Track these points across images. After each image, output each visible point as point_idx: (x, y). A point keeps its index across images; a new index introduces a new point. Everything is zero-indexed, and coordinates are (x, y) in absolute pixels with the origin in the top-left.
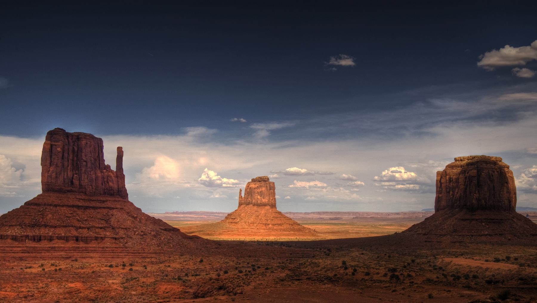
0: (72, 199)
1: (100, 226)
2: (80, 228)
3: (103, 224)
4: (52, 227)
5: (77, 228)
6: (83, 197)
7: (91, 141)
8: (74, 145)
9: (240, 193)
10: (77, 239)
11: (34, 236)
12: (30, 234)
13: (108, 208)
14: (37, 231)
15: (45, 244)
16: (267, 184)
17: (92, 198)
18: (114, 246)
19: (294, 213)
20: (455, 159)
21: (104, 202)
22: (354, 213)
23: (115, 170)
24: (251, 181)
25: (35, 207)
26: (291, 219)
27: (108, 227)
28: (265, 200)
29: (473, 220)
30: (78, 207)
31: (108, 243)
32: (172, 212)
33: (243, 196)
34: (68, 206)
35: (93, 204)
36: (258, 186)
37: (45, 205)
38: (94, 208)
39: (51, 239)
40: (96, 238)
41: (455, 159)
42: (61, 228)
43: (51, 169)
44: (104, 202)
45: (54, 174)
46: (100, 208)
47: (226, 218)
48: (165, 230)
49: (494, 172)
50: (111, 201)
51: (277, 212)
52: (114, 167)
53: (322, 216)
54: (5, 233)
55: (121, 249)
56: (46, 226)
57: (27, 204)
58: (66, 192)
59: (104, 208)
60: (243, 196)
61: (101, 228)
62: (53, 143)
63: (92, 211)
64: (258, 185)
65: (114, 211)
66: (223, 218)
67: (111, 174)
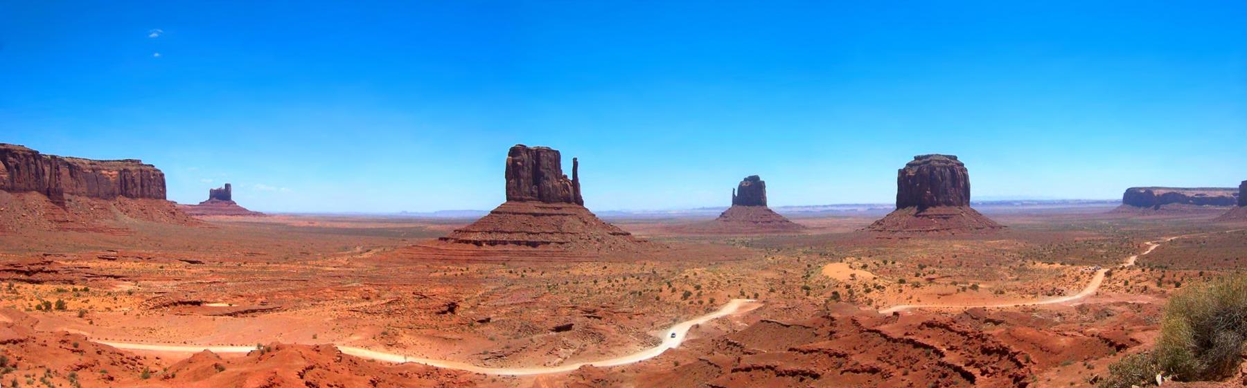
1: (550, 231)
2: (533, 233)
4: (505, 232)
5: (529, 233)
6: (541, 204)
9: (734, 192)
10: (528, 244)
11: (490, 241)
12: (488, 239)
13: (563, 215)
14: (494, 236)
15: (499, 247)
18: (557, 249)
19: (813, 207)
20: (915, 157)
21: (558, 209)
22: (869, 205)
23: (571, 179)
25: (498, 215)
26: (781, 216)
27: (557, 232)
29: (924, 216)
30: (535, 215)
31: (551, 248)
32: (699, 207)
35: (549, 211)
37: (507, 213)
38: (549, 215)
39: (505, 243)
40: (543, 243)
41: (915, 157)
43: (513, 181)
44: (558, 209)
46: (555, 215)
47: (721, 216)
48: (614, 234)
49: (946, 171)
52: (570, 178)
53: (839, 209)
54: (468, 238)
55: (560, 253)
56: (502, 232)
57: (492, 212)
59: (559, 214)
61: (550, 233)
63: (548, 217)
65: (567, 217)
66: (718, 217)
67: (568, 184)
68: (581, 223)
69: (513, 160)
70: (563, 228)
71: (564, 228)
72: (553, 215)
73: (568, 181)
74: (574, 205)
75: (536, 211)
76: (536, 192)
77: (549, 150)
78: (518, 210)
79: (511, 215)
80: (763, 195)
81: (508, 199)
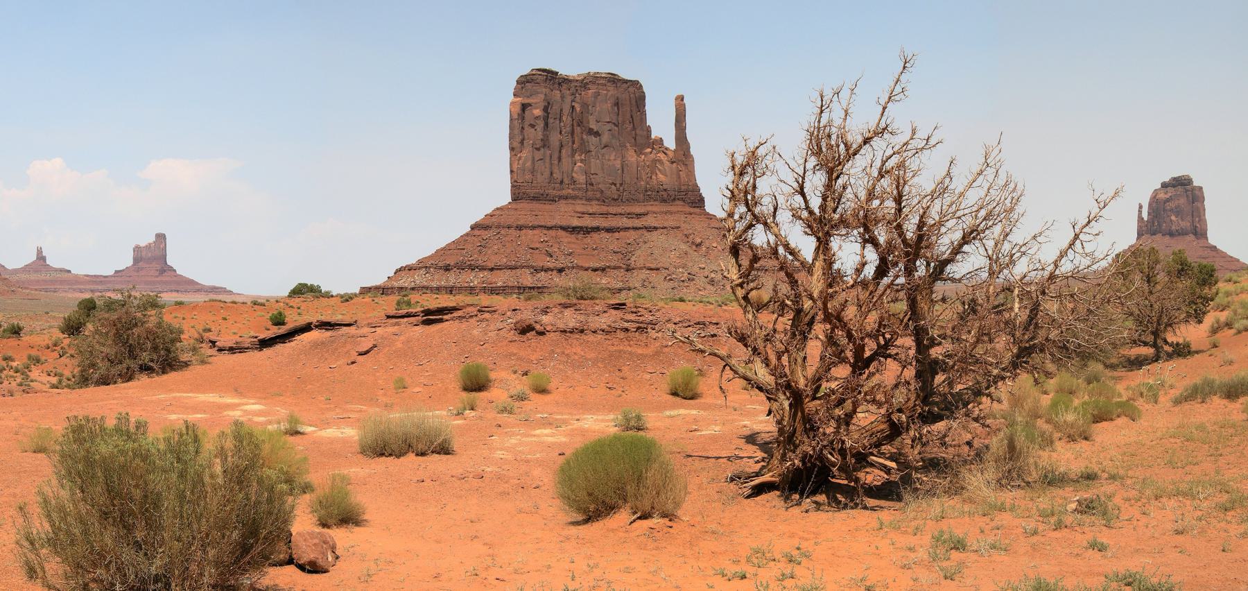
0: (565, 213)
1: (597, 265)
3: (614, 260)
4: (482, 269)
6: (595, 207)
7: (609, 88)
8: (573, 101)
9: (1140, 212)
13: (646, 228)
16: (1187, 191)
17: (612, 210)
21: (639, 216)
24: (1160, 187)
25: (482, 232)
27: (615, 268)
28: (1185, 224)
33: (1146, 219)
34: (545, 227)
36: (1171, 197)
38: (609, 230)
42: (502, 271)
43: (524, 155)
44: (639, 216)
45: (529, 164)
50: (654, 213)
51: (1207, 247)
52: (670, 143)
57: (473, 228)
58: (557, 199)
60: (1145, 216)
62: (526, 101)
63: (608, 235)
64: (1170, 194)
65: (655, 233)
68: (684, 247)
69: (524, 107)
70: (633, 259)
71: (638, 258)
72: (618, 230)
73: (665, 151)
74: (678, 206)
75: (576, 222)
76: (581, 178)
77: (613, 79)
78: (531, 220)
79: (512, 231)
80: (1200, 217)
81: (516, 197)
